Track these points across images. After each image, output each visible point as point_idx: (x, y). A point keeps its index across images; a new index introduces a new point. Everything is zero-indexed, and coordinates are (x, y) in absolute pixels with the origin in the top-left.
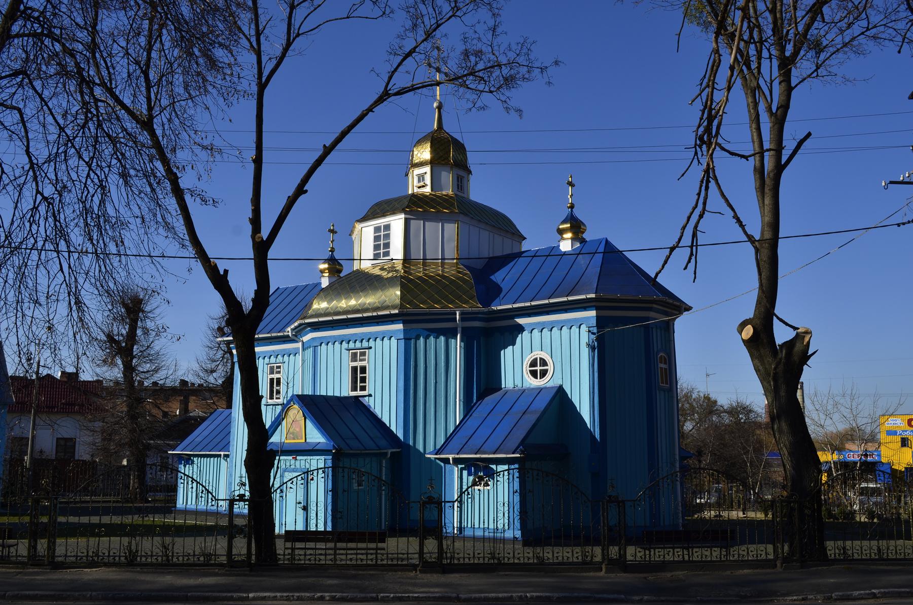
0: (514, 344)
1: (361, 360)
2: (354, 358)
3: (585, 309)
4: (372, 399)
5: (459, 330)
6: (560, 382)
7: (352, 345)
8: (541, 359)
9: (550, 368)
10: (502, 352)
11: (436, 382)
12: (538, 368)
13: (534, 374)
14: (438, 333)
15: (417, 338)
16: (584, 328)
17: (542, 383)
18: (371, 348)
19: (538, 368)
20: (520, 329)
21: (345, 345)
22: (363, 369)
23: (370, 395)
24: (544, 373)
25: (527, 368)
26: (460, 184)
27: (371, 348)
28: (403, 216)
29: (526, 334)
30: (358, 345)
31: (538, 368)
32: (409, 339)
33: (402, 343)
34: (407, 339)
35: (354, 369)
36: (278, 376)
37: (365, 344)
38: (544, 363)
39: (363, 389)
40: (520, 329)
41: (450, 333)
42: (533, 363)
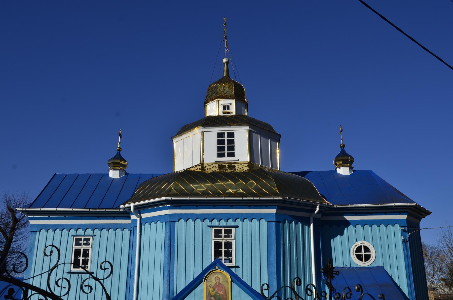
0: (342, 234)
1: (225, 237)
2: (218, 233)
3: (400, 213)
4: (240, 270)
5: (312, 219)
7: (215, 223)
8: (365, 247)
9: (373, 252)
10: (332, 240)
11: (297, 259)
14: (297, 219)
15: (284, 222)
16: (398, 228)
17: (370, 263)
18: (238, 227)
19: (363, 253)
20: (347, 223)
21: (207, 222)
22: (228, 245)
23: (238, 267)
24: (367, 258)
25: (353, 254)
27: (238, 227)
28: (248, 128)
29: (351, 227)
30: (223, 223)
31: (363, 253)
32: (279, 221)
33: (274, 224)
34: (277, 222)
35: (218, 245)
36: (86, 247)
37: (231, 223)
40: (347, 223)
41: (306, 222)
42: (359, 249)
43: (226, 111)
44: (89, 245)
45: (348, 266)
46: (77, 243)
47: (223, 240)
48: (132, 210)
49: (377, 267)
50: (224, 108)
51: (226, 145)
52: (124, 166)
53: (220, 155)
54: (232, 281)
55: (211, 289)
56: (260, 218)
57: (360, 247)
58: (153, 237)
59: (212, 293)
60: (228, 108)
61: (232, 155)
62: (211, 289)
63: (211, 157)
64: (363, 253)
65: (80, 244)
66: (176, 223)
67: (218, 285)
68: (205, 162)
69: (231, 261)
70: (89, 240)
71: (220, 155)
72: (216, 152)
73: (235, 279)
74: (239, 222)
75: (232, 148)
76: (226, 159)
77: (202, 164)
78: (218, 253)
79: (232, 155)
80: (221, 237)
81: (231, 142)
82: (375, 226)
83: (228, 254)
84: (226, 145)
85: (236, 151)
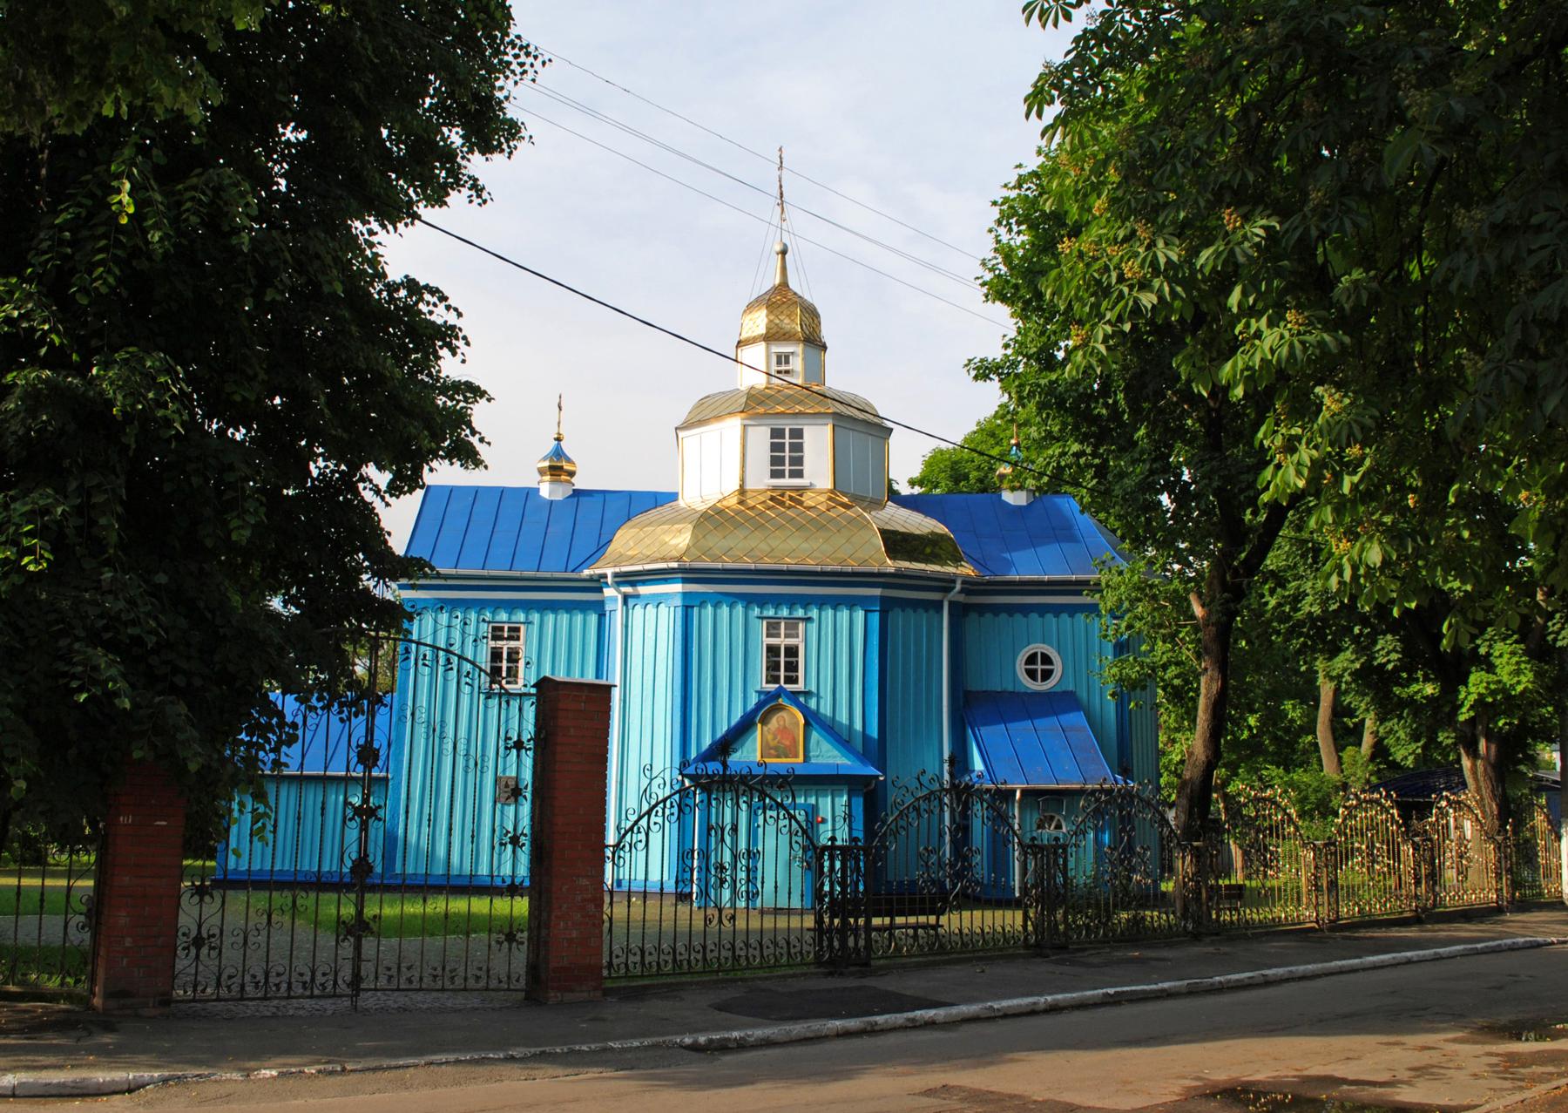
1: (787, 636)
2: (773, 630)
6: (1071, 688)
12: (1039, 667)
13: (1032, 674)
18: (809, 620)
22: (792, 651)
24: (1047, 675)
25: (1021, 667)
26: (816, 370)
27: (809, 620)
31: (1039, 667)
35: (773, 651)
38: (1046, 659)
39: (792, 680)
42: (1031, 659)
43: (783, 368)
44: (518, 639)
45: (1010, 689)
46: (495, 638)
47: (782, 641)
48: (609, 580)
49: (1065, 693)
50: (779, 363)
51: (787, 454)
52: (572, 474)
53: (776, 474)
54: (807, 724)
55: (770, 737)
56: (851, 603)
57: (1035, 654)
58: (650, 634)
59: (772, 744)
60: (787, 362)
61: (799, 474)
62: (770, 737)
63: (761, 480)
64: (1039, 666)
65: (501, 638)
66: (696, 610)
67: (783, 730)
68: (748, 487)
69: (795, 681)
70: (518, 630)
71: (776, 474)
72: (768, 468)
73: (812, 719)
74: (814, 613)
75: (798, 461)
76: (787, 481)
77: (742, 491)
78: (773, 667)
79: (799, 474)
80: (778, 636)
81: (797, 448)
82: (1064, 616)
83: (792, 667)
84: (787, 454)
85: (807, 467)
